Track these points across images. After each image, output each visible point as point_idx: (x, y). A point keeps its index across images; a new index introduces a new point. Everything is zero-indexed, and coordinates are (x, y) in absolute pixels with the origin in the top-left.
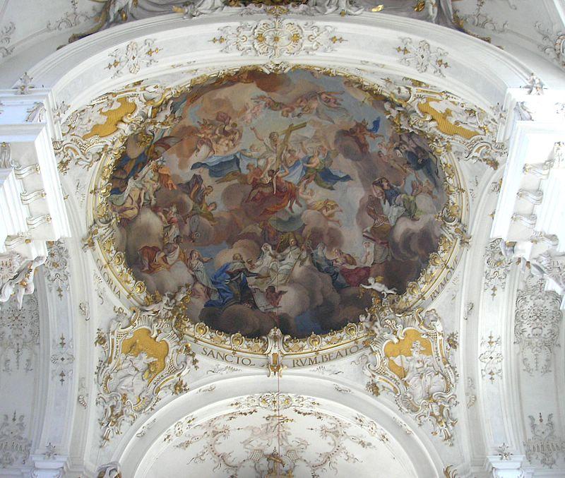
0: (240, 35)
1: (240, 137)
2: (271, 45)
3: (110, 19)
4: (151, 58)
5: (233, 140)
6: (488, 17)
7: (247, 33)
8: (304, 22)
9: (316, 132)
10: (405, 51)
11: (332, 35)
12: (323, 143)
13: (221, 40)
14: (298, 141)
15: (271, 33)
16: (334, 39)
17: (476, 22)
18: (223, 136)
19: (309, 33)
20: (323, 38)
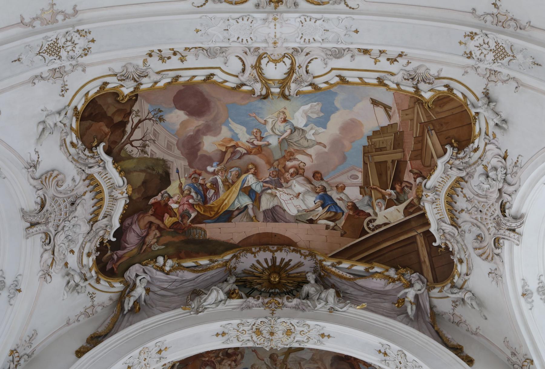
0: (240, 330)
1: (242, 357)
2: (267, 337)
3: (125, 310)
4: (161, 356)
5: (235, 361)
6: (462, 318)
7: (246, 328)
8: (296, 321)
9: (313, 355)
10: (385, 354)
11: (322, 332)
12: (319, 365)
13: (224, 334)
14: (296, 361)
15: (268, 329)
16: (323, 335)
17: (452, 320)
18: (226, 358)
19: (301, 329)
20: (314, 334)
